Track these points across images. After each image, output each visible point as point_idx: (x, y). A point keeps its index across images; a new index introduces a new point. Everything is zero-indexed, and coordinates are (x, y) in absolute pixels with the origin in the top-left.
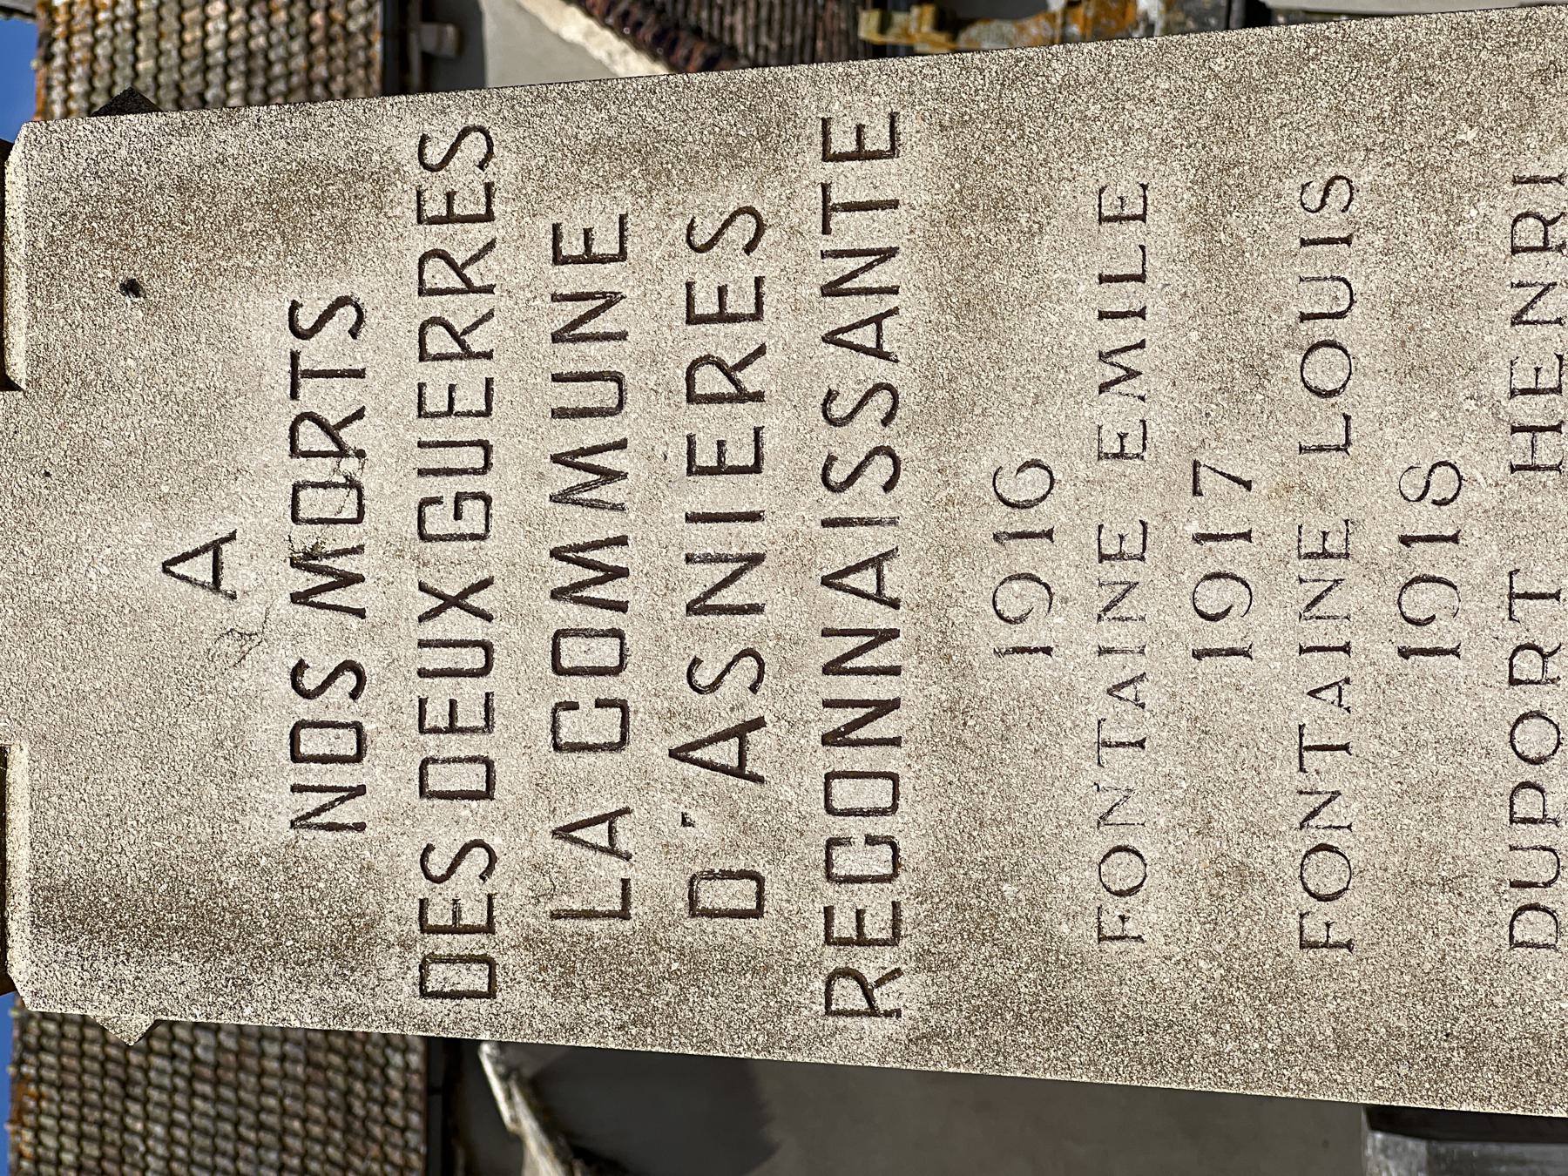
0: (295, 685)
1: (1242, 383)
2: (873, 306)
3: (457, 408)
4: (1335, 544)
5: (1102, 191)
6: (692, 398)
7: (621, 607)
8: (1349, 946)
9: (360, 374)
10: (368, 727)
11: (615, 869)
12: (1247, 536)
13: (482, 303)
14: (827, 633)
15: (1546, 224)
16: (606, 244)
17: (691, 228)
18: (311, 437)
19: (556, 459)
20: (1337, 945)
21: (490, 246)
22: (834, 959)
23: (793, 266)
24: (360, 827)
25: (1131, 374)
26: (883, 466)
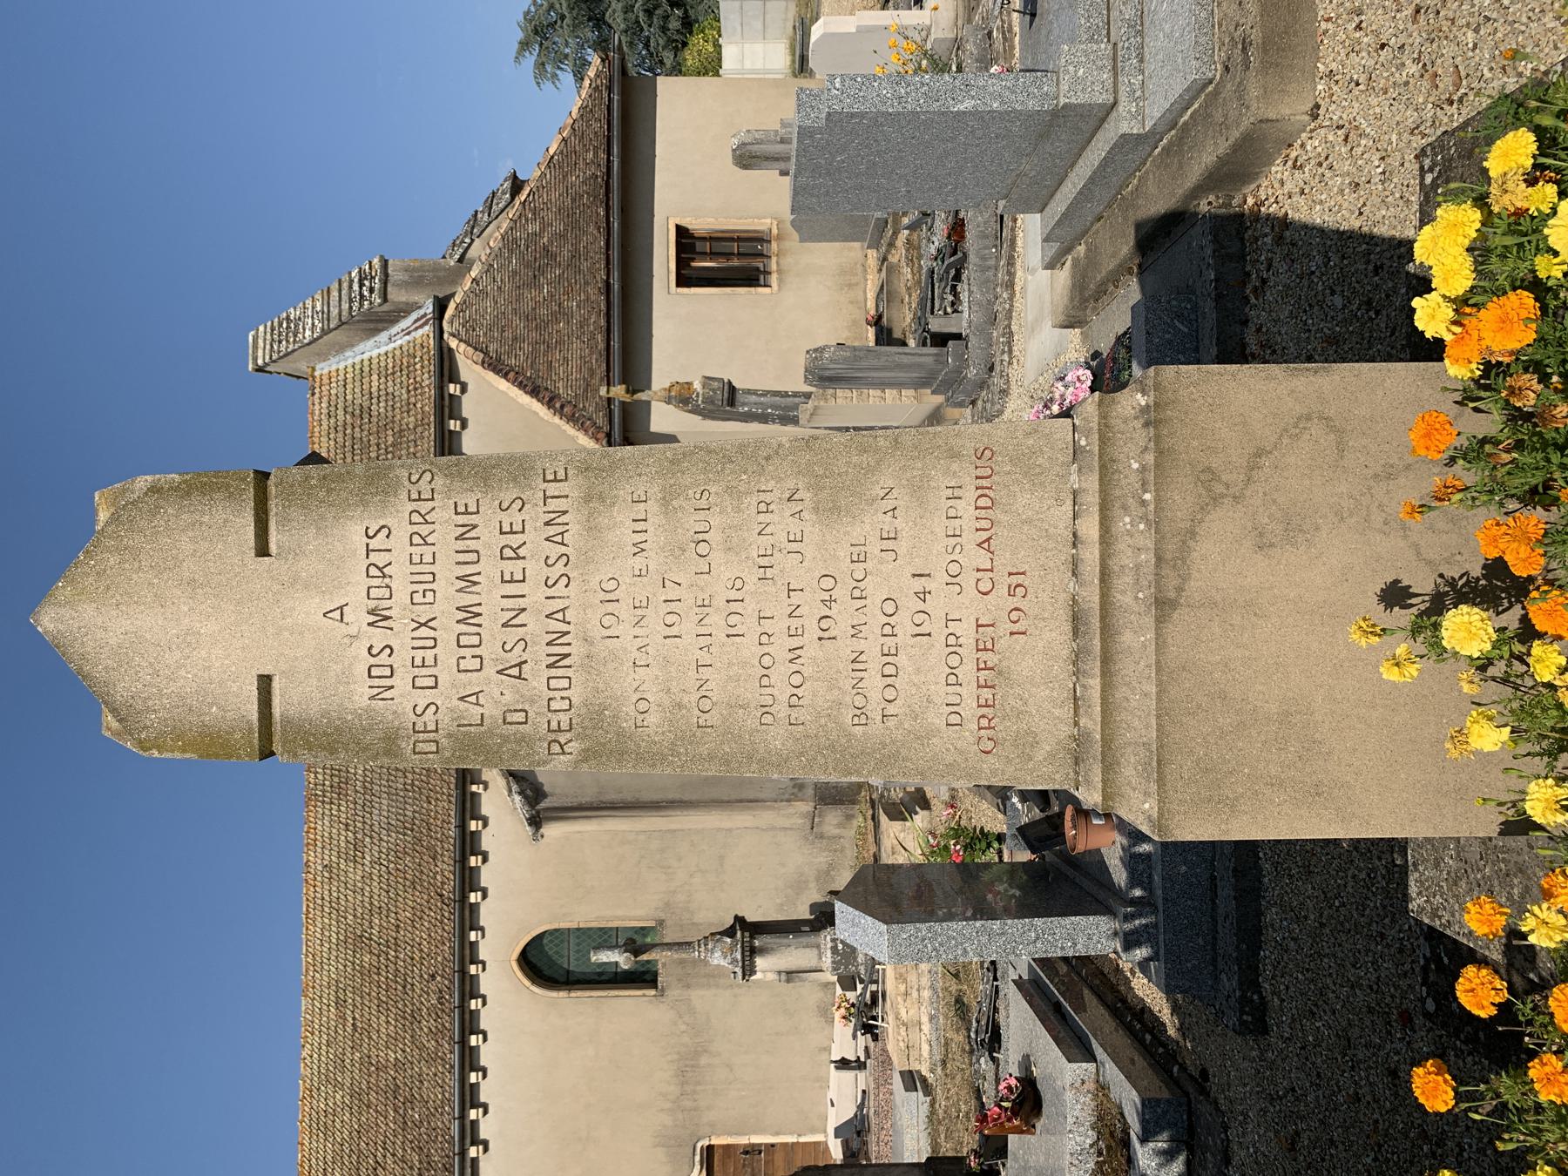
1: (678, 553)
11: (481, 710)
16: (472, 508)
22: (552, 736)
26: (564, 580)
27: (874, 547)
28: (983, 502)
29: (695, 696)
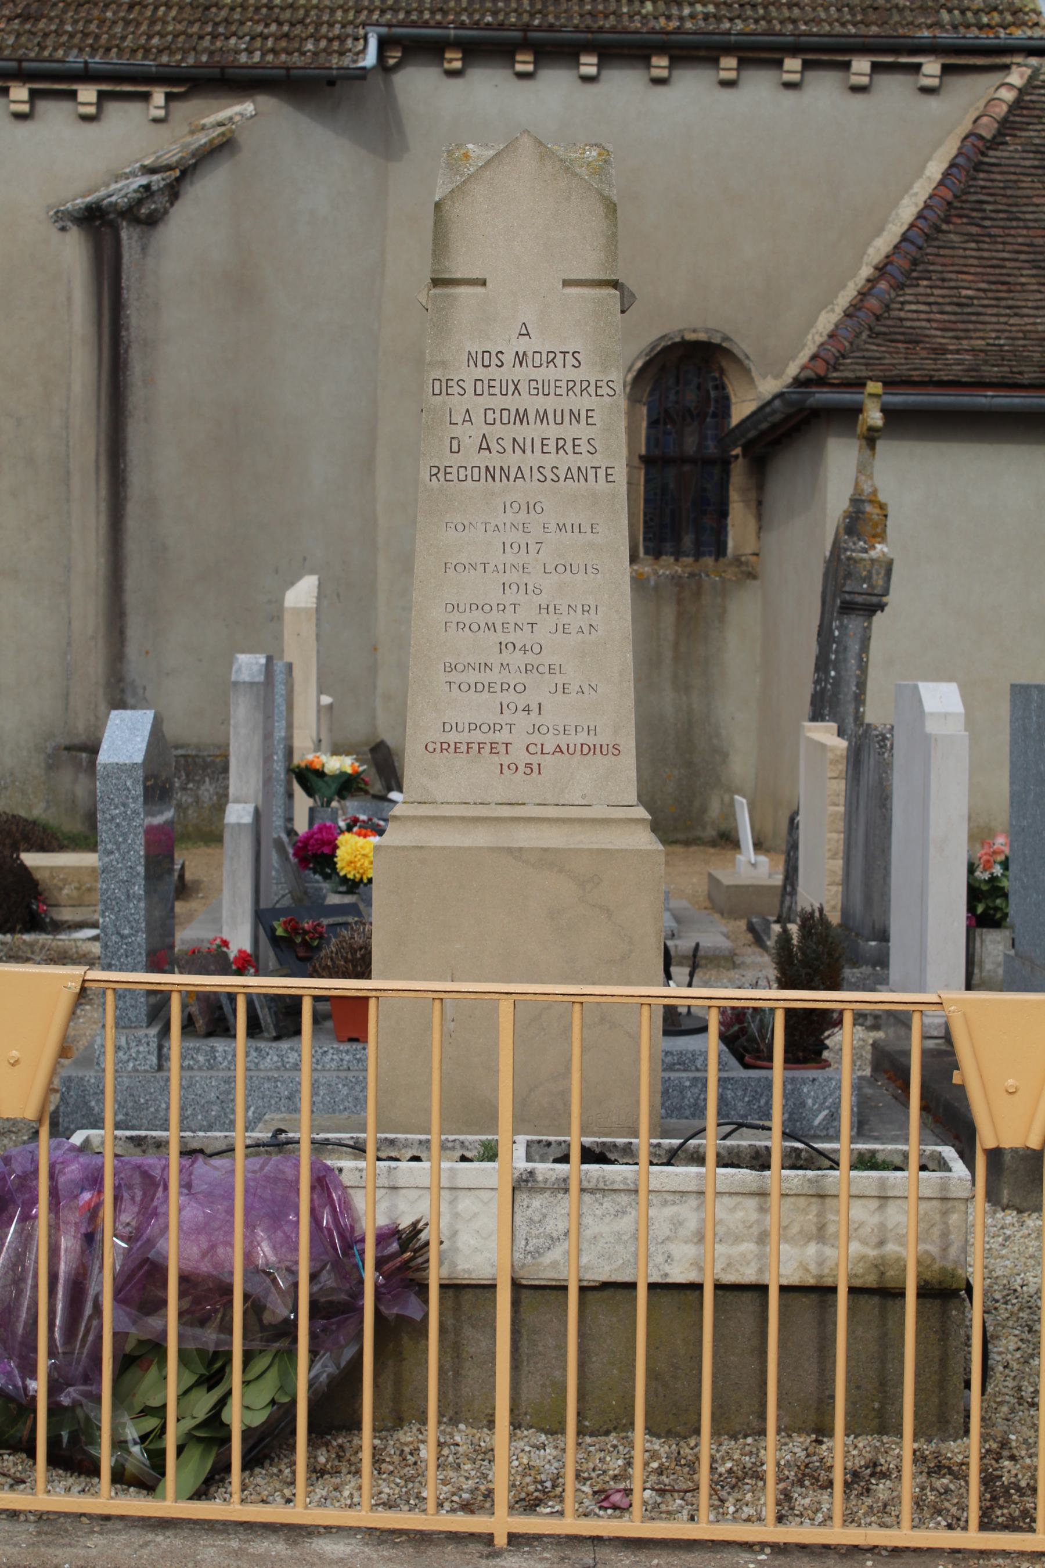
11: (460, 422)
16: (590, 421)
18: (551, 356)
23: (584, 461)
27: (560, 679)
28: (586, 749)
29: (464, 561)
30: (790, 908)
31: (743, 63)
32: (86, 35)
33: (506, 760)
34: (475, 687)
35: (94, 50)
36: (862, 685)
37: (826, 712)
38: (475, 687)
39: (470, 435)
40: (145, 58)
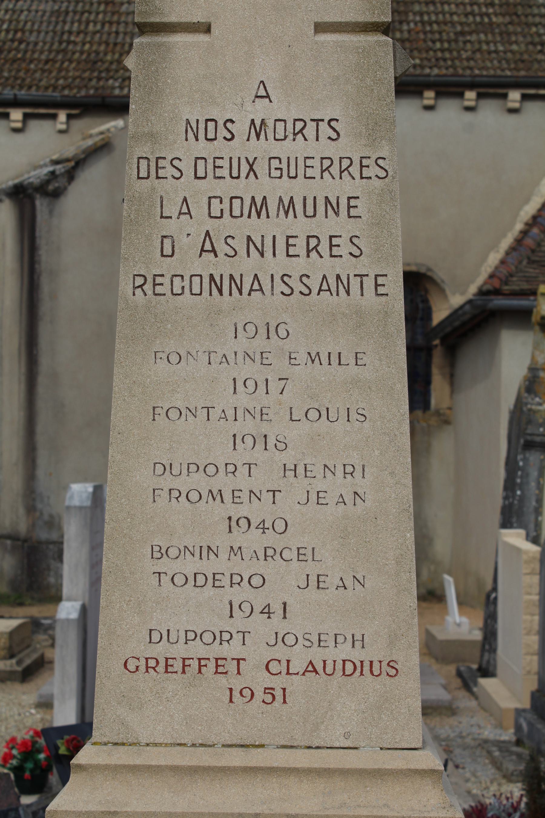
0: (228, 120)
2: (334, 290)
3: (307, 169)
4: (265, 417)
5: (364, 353)
6: (308, 237)
7: (249, 216)
8: (154, 420)
9: (317, 140)
10: (215, 142)
11: (175, 215)
12: (267, 393)
13: (337, 177)
14: (241, 275)
15: (351, 474)
16: (353, 212)
17: (357, 237)
18: (299, 125)
19: (292, 198)
20: (154, 416)
21: (354, 178)
23: (345, 266)
24: (187, 140)
25: (313, 361)
26: (288, 291)
27: (313, 569)
28: (349, 667)
29: (179, 404)
30: (488, 662)
31: (439, 95)
32: (16, 78)
33: (237, 684)
34: (195, 580)
35: (21, 87)
36: (539, 501)
37: (514, 520)
38: (195, 580)
39: (188, 233)
40: (54, 91)
